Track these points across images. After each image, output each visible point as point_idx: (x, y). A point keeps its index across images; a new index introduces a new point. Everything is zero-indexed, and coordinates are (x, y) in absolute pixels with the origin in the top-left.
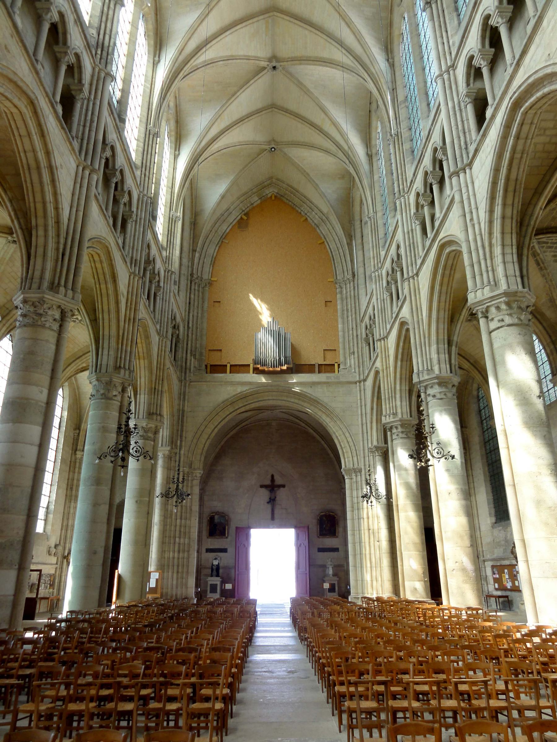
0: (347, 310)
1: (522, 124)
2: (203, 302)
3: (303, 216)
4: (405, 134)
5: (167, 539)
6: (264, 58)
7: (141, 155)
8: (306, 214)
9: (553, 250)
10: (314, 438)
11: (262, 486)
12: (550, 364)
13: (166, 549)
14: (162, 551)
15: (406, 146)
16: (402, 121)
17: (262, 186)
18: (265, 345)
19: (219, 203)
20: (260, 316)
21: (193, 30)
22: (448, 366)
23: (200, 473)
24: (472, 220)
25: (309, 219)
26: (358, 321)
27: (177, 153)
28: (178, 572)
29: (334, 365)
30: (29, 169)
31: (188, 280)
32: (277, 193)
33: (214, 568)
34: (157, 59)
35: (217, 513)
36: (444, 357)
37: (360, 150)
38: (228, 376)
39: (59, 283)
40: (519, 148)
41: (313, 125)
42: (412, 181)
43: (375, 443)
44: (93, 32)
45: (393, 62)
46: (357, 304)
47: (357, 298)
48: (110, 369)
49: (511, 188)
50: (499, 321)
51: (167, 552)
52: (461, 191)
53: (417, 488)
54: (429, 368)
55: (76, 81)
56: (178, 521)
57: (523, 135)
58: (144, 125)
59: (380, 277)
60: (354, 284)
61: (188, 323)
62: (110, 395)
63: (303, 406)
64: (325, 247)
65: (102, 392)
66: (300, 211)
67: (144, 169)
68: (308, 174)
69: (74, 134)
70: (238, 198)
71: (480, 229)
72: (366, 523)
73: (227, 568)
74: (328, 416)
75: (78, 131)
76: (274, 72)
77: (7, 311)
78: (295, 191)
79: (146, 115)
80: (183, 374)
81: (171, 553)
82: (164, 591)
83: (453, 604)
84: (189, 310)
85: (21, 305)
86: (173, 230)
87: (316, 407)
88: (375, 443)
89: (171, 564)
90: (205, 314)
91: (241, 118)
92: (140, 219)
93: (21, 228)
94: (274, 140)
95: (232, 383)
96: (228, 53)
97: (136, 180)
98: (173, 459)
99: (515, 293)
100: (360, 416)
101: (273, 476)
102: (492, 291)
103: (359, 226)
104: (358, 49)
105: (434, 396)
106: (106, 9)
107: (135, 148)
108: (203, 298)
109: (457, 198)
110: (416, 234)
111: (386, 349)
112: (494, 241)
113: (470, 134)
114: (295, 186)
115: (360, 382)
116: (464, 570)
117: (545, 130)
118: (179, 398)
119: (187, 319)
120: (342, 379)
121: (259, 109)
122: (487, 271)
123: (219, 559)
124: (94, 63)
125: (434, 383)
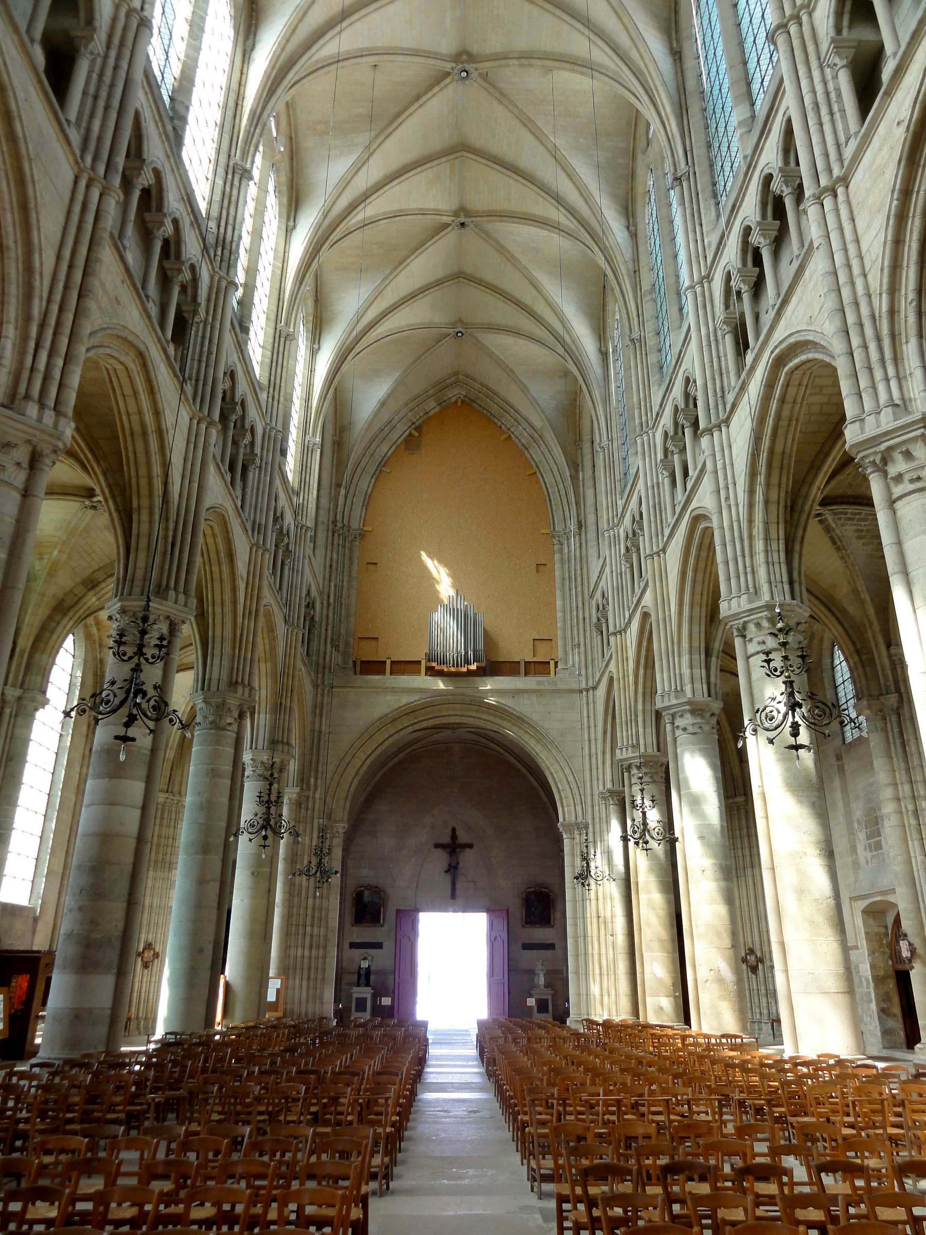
0: (570, 578)
1: (787, 385)
2: (351, 564)
4: (651, 341)
5: (294, 928)
6: (447, 211)
7: (268, 369)
9: (855, 522)
10: (518, 770)
11: (437, 846)
12: (854, 682)
13: (293, 944)
14: (286, 947)
15: (653, 359)
16: (648, 321)
17: (441, 386)
18: (443, 631)
19: (377, 413)
20: (437, 587)
21: (345, 183)
22: (705, 686)
23: (344, 827)
24: (727, 498)
25: (513, 436)
26: (586, 596)
27: (316, 346)
28: (309, 979)
29: (549, 663)
30: (132, 434)
32: (465, 396)
33: (363, 972)
35: (368, 887)
36: (700, 672)
37: (588, 345)
38: (389, 680)
39: (167, 586)
40: (786, 413)
41: (518, 304)
42: (658, 414)
43: (609, 785)
44: (212, 225)
45: (636, 230)
47: (583, 560)
48: (223, 686)
49: (776, 463)
50: (759, 643)
51: (292, 949)
52: (714, 455)
53: (666, 857)
54: (679, 688)
55: (189, 298)
56: (310, 901)
57: (789, 398)
58: (272, 325)
59: (617, 538)
60: (580, 540)
61: (329, 597)
62: (223, 724)
63: (501, 726)
64: (537, 481)
65: (211, 718)
66: (499, 424)
67: (271, 390)
68: (512, 371)
70: (406, 405)
71: (738, 514)
72: (594, 908)
73: (382, 973)
74: (538, 741)
75: (191, 368)
77: (76, 599)
79: (275, 309)
80: (320, 676)
81: (300, 950)
82: (289, 1006)
83: (705, 1030)
85: (118, 616)
86: (309, 465)
87: (520, 728)
88: (609, 785)
89: (298, 966)
90: (354, 583)
91: (413, 292)
92: (266, 463)
93: (117, 510)
94: (461, 321)
95: (394, 691)
96: (395, 207)
97: (260, 407)
98: (303, 806)
100: (587, 743)
102: (750, 601)
103: (590, 450)
104: (585, 211)
105: (685, 729)
106: (228, 189)
107: (259, 358)
108: (351, 558)
110: (664, 491)
111: (624, 648)
112: (755, 532)
113: (728, 377)
114: (494, 388)
115: (587, 690)
116: (720, 980)
117: (821, 388)
118: (314, 713)
119: (326, 590)
120: (560, 686)
121: (440, 280)
122: (746, 574)
123: (370, 958)
124: (213, 269)
125: (685, 711)
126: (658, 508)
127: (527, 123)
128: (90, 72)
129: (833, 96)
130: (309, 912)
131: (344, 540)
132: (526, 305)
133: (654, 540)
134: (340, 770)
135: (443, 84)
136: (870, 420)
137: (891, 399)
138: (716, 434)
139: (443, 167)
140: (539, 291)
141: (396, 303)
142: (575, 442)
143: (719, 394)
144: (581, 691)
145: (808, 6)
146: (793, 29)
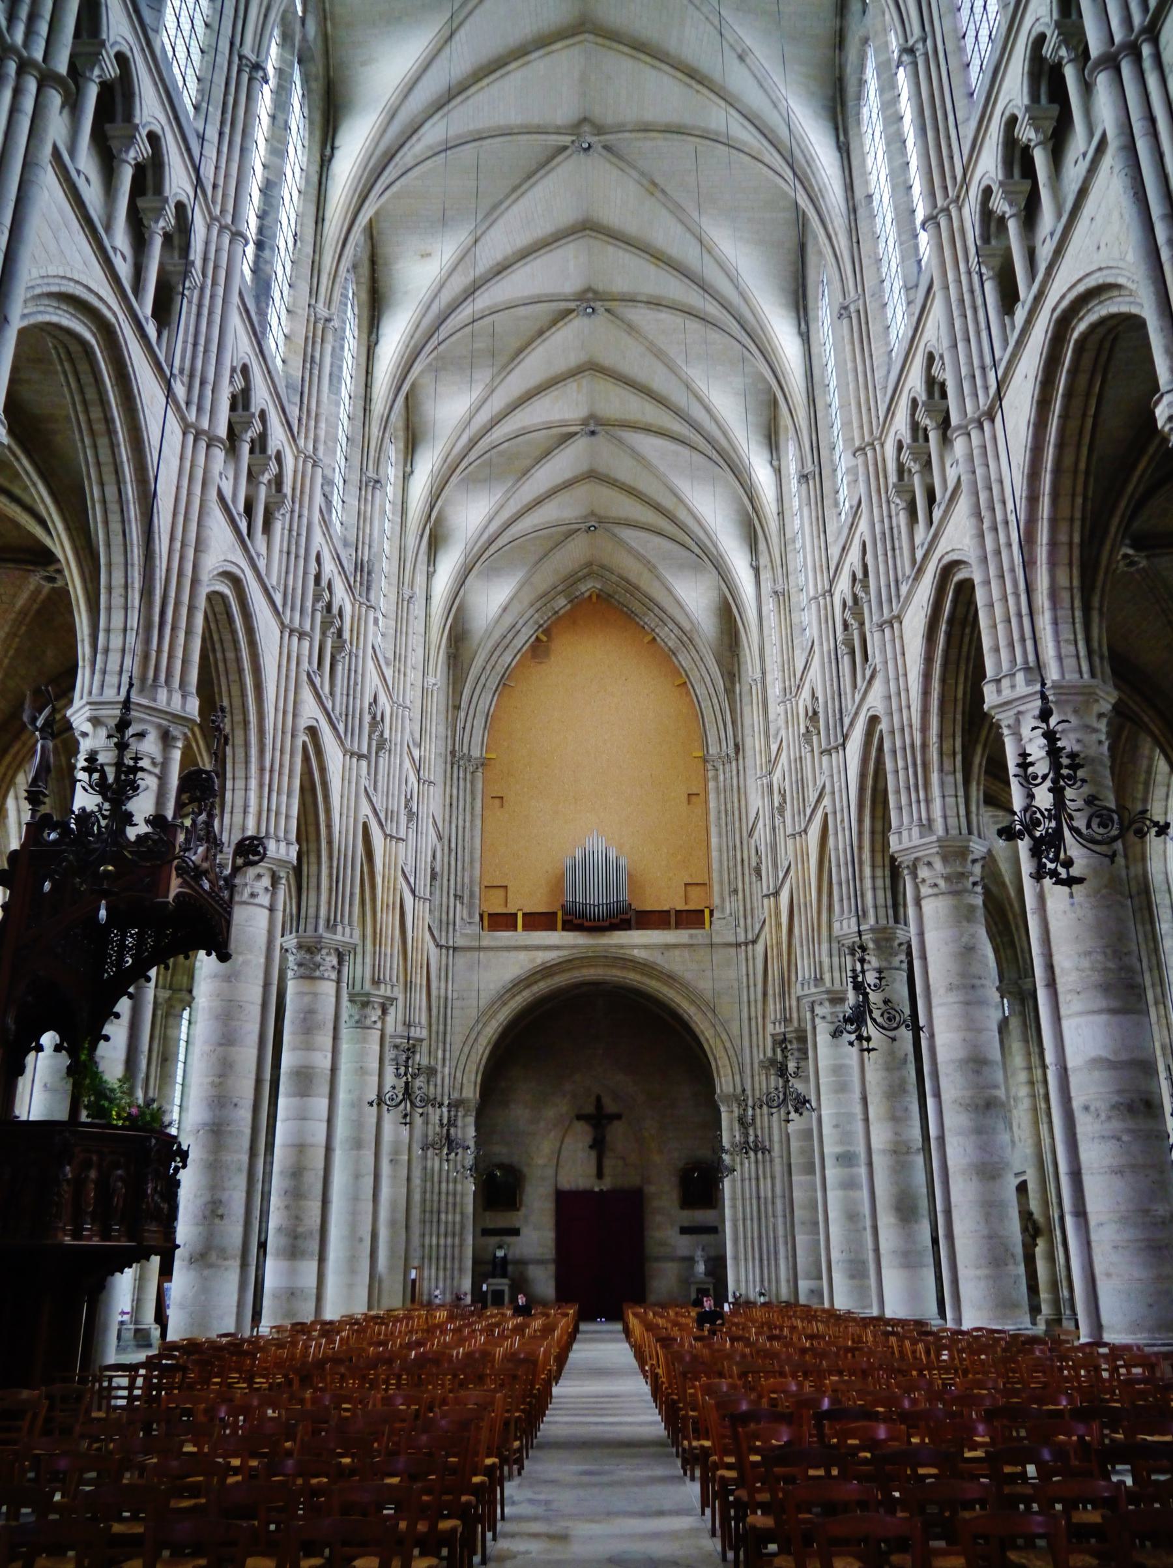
3: (648, 634)
11: (579, 1117)
17: (572, 580)
24: (842, 821)
26: (745, 835)
28: (445, 1269)
29: (703, 911)
32: (601, 590)
34: (408, 469)
35: (501, 1166)
43: (769, 1054)
46: (743, 803)
56: (444, 1185)
61: (450, 841)
64: (688, 693)
65: (357, 1017)
69: (337, 712)
73: (522, 1263)
75: (341, 704)
76: (593, 438)
78: (633, 588)
85: (295, 951)
94: (593, 514)
99: (884, 929)
101: (599, 1099)
105: (824, 1018)
109: (828, 789)
114: (634, 580)
115: (746, 944)
126: (801, 784)
127: (659, 354)
128: (283, 529)
130: (443, 1197)
133: (796, 819)
134: (471, 1041)
135: (566, 320)
136: (905, 834)
137: (920, 819)
138: (834, 755)
139: (572, 386)
140: (681, 500)
142: (731, 647)
143: (838, 716)
144: (738, 945)
145: (880, 438)
146: (870, 454)
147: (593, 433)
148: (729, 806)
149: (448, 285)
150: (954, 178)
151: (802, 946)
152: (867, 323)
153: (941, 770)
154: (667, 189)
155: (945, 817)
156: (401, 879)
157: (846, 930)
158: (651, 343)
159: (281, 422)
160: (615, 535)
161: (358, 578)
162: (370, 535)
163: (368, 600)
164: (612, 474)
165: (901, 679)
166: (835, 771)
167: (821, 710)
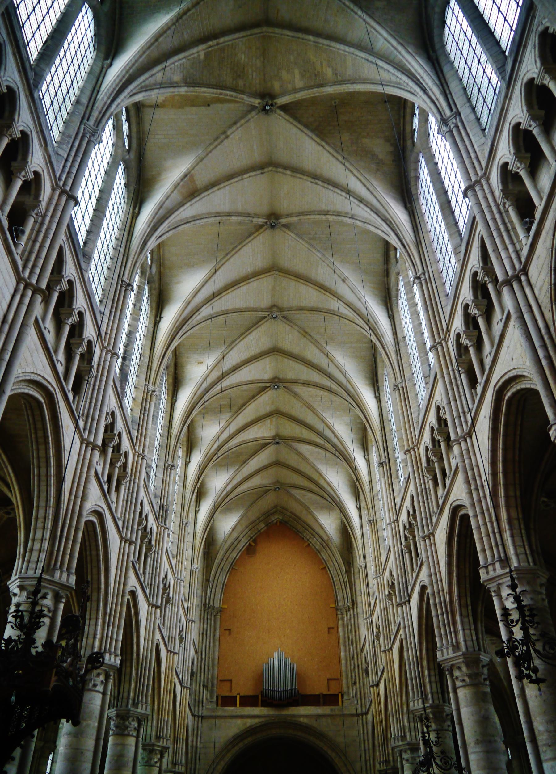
3: (305, 542)
8: (308, 540)
17: (267, 515)
24: (411, 643)
26: (359, 650)
29: (338, 695)
31: (201, 610)
32: (282, 520)
34: (188, 460)
64: (327, 573)
65: (146, 759)
69: (146, 583)
70: (247, 527)
75: (149, 578)
78: (298, 519)
84: (203, 640)
85: (114, 718)
91: (251, 474)
92: (175, 600)
94: (278, 482)
114: (298, 514)
115: (362, 715)
121: (266, 465)
126: (387, 622)
127: (309, 407)
128: (125, 489)
129: (428, 490)
131: (211, 615)
132: (314, 480)
135: (265, 391)
136: (445, 651)
137: (452, 642)
138: (404, 607)
139: (268, 421)
140: (321, 475)
141: (241, 481)
144: (357, 715)
145: (417, 446)
146: (412, 453)
147: (278, 443)
148: (350, 634)
149: (210, 376)
150: (443, 329)
151: (393, 716)
152: (407, 393)
153: (461, 615)
154: (312, 334)
155: (465, 641)
156: (175, 676)
157: (417, 707)
158: (305, 401)
159: (128, 438)
160: (288, 492)
161: (161, 514)
162: (168, 492)
163: (165, 525)
164: (287, 463)
165: (436, 566)
166: (405, 615)
167: (396, 582)
